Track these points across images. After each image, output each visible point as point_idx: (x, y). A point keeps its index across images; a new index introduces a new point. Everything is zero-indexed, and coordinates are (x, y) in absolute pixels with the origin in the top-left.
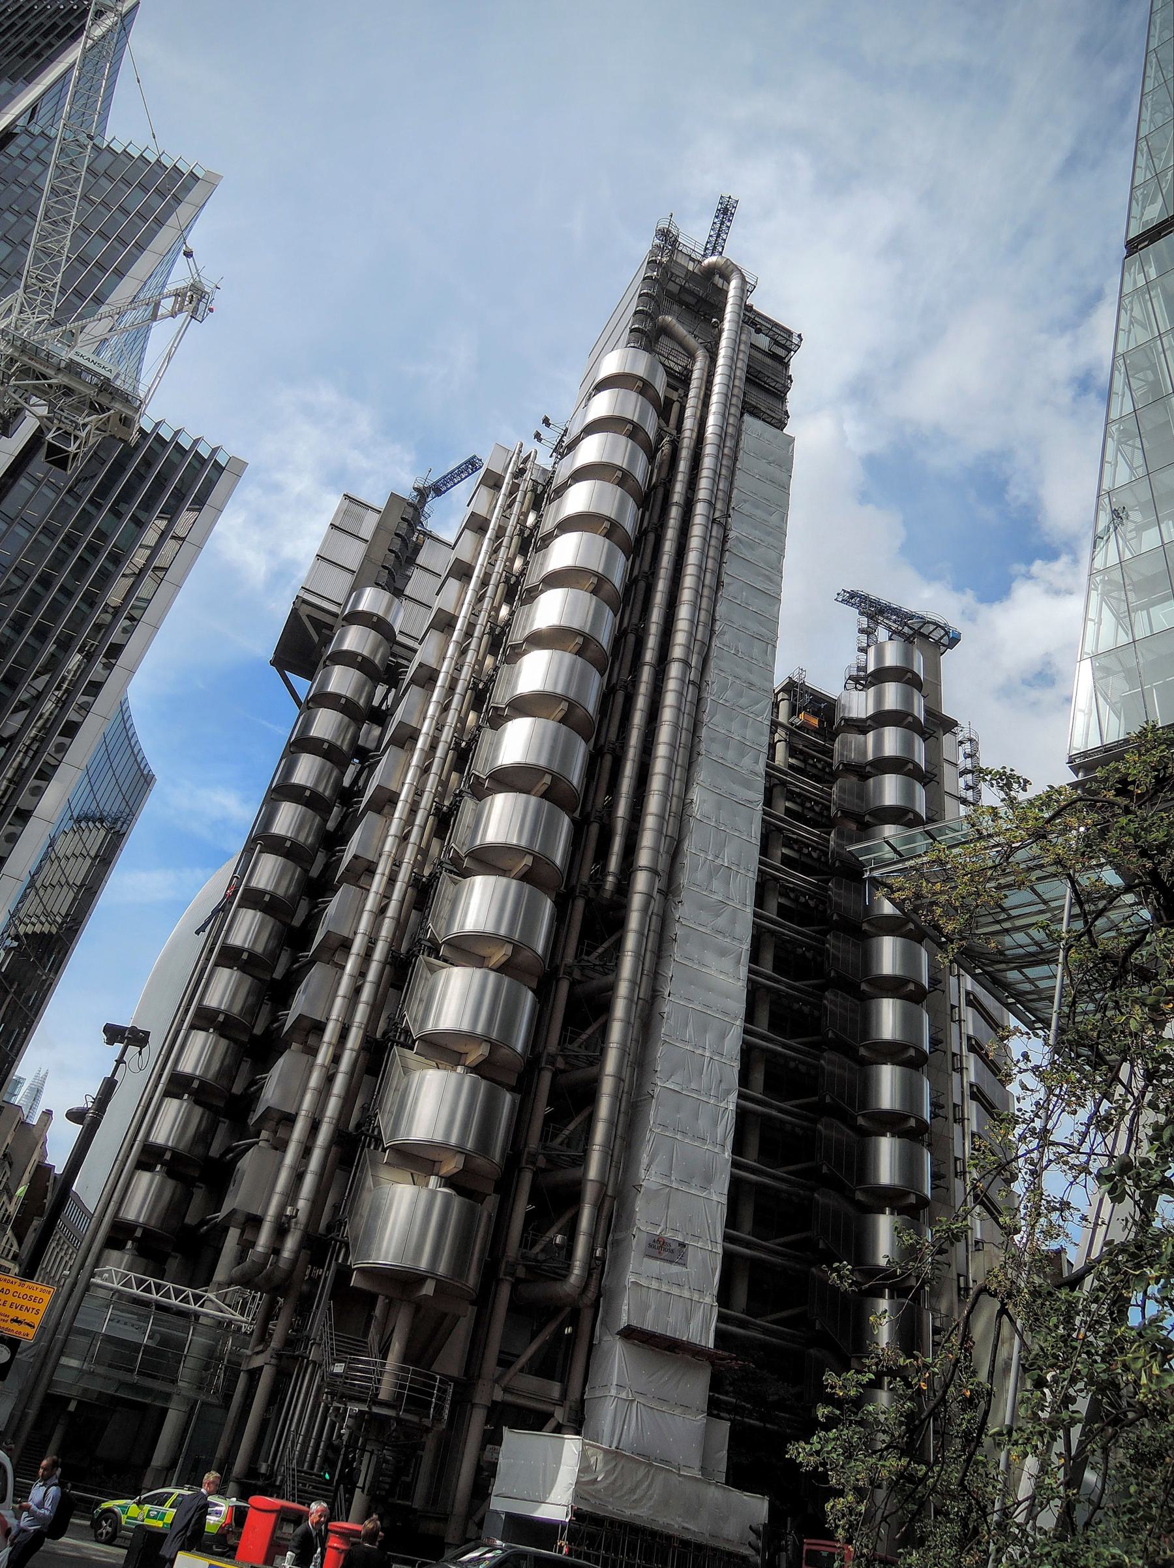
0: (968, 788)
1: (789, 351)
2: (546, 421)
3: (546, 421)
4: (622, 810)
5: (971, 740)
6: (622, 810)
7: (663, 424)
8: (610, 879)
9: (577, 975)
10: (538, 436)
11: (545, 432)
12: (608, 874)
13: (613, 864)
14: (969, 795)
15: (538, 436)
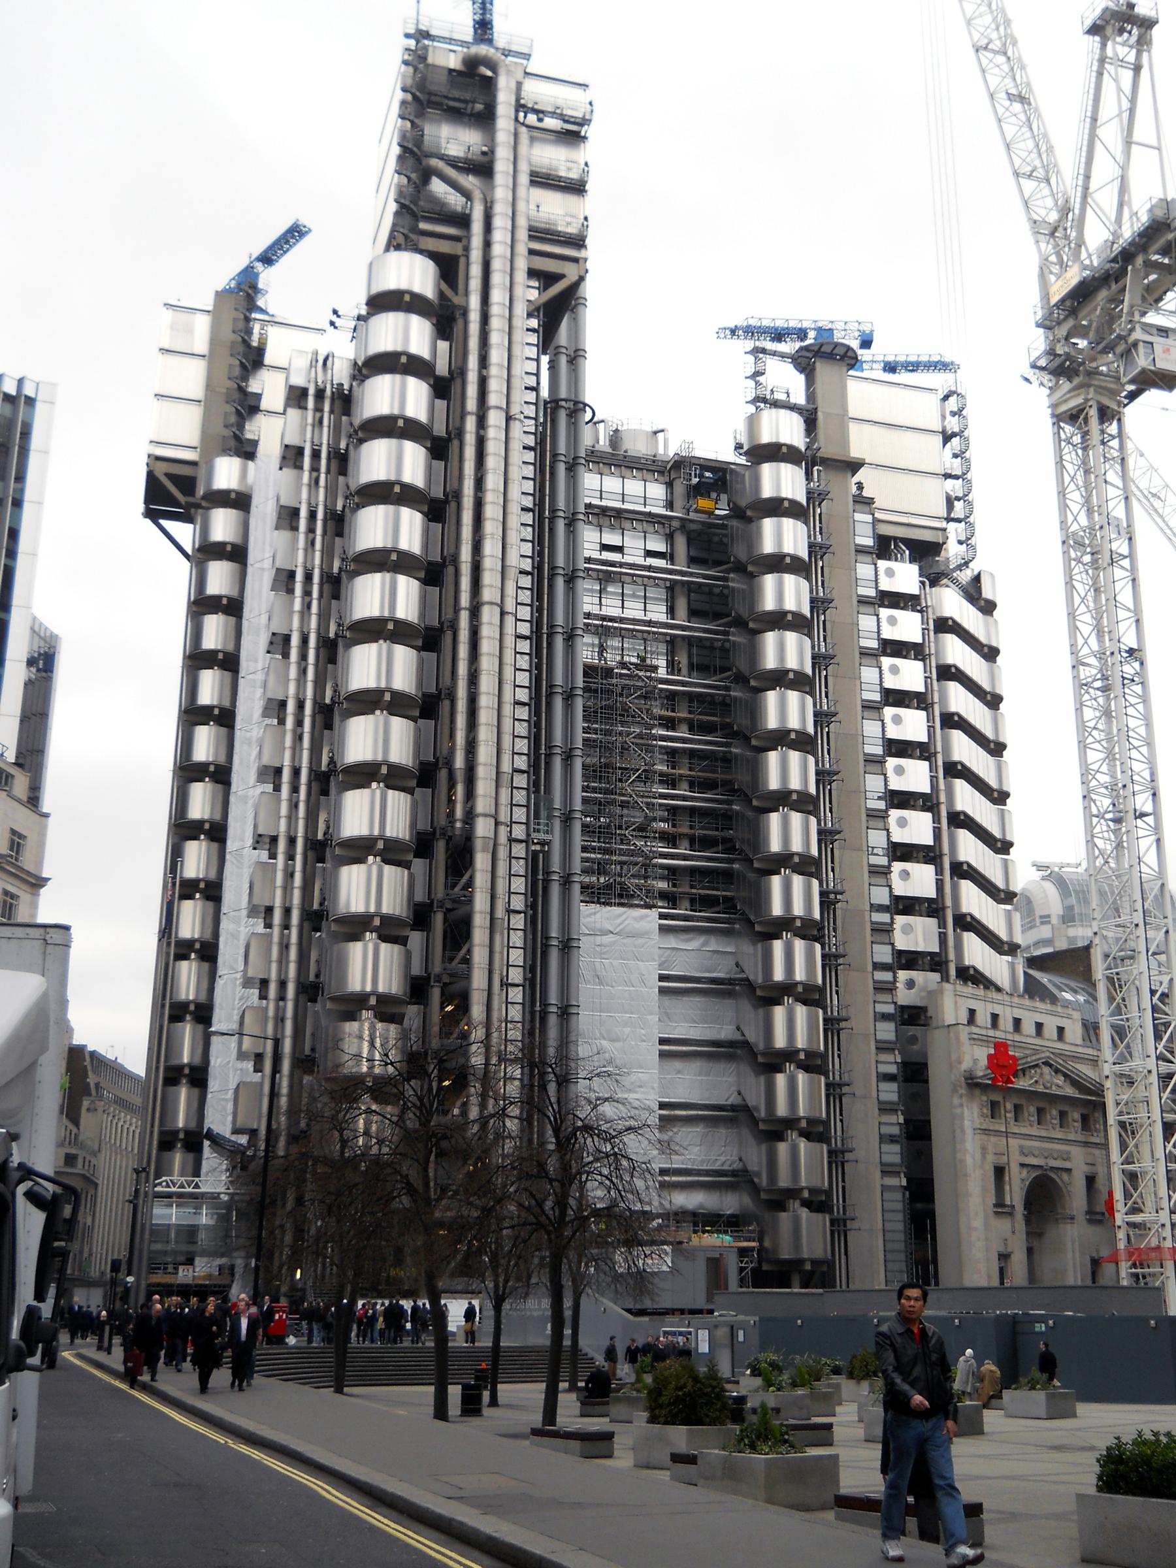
0: (955, 456)
1: (582, 125)
2: (335, 312)
3: (335, 312)
4: (459, 762)
5: (955, 392)
6: (459, 762)
7: (449, 292)
8: (458, 825)
9: (449, 905)
10: (332, 323)
11: (338, 322)
12: (455, 821)
13: (459, 813)
14: (956, 466)
15: (332, 323)
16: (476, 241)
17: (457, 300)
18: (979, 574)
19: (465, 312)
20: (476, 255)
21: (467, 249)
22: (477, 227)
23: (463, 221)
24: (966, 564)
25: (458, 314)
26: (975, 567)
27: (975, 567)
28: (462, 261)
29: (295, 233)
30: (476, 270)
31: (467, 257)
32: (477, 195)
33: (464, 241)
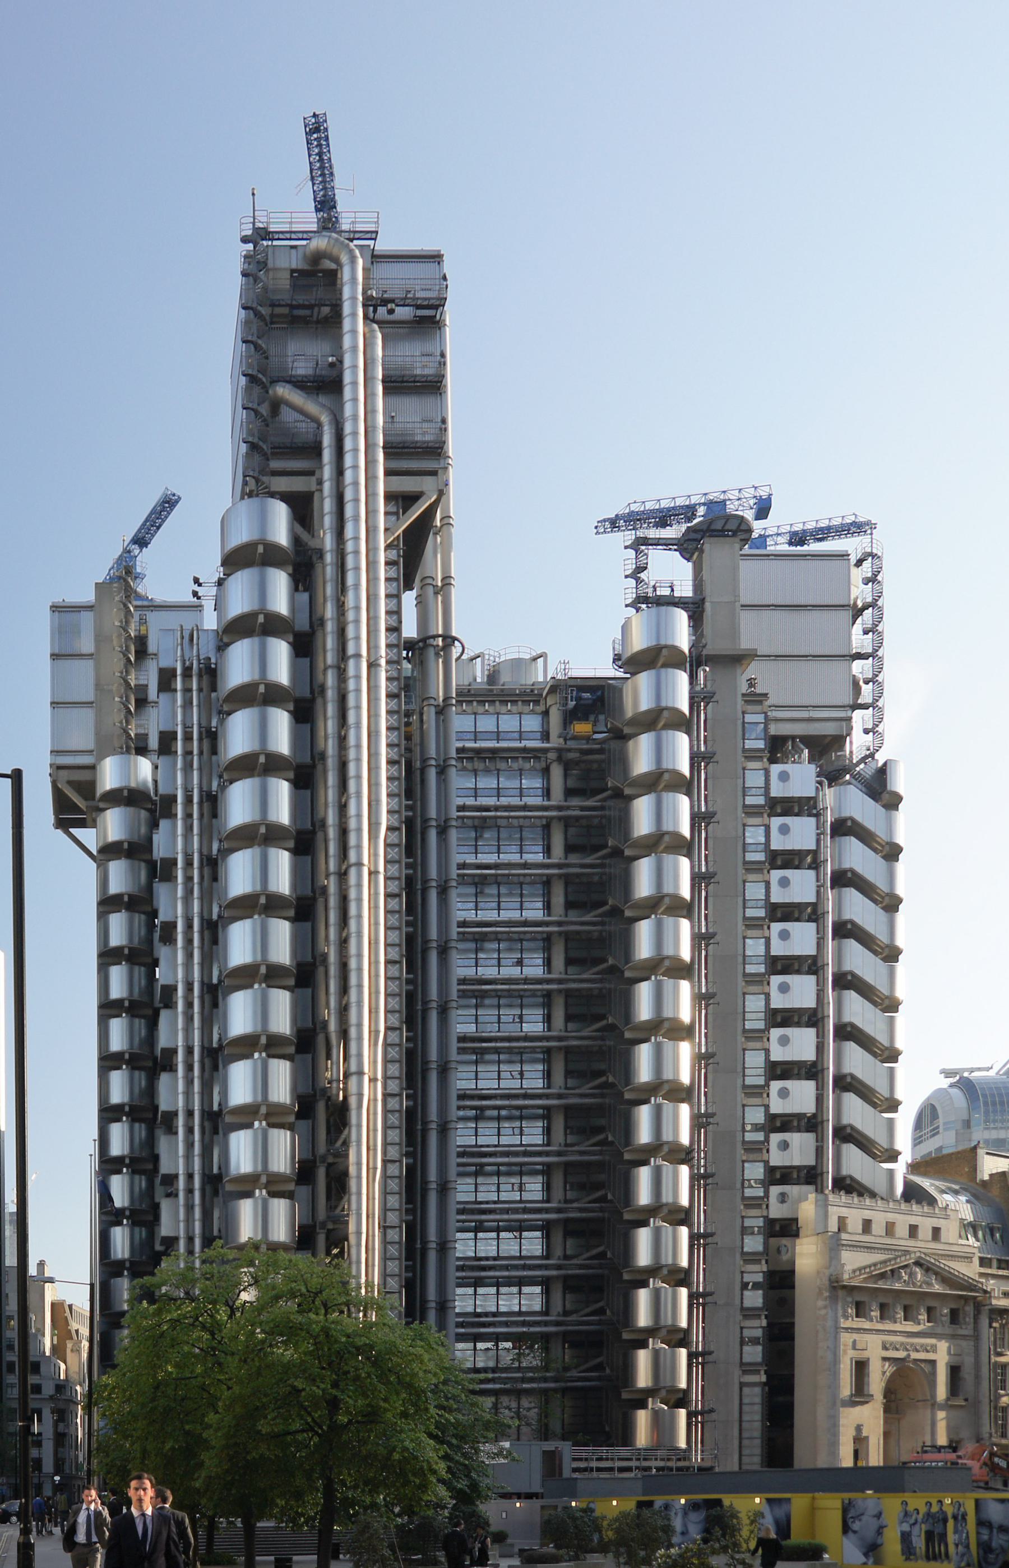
16: (327, 472)
17: (313, 543)
18: (885, 764)
19: (320, 554)
20: (327, 487)
21: (320, 482)
22: (327, 455)
23: (316, 450)
24: (872, 756)
25: (314, 558)
26: (881, 758)
27: (881, 758)
28: (316, 496)
29: (168, 504)
30: (328, 505)
31: (321, 490)
32: (325, 419)
33: (317, 472)
